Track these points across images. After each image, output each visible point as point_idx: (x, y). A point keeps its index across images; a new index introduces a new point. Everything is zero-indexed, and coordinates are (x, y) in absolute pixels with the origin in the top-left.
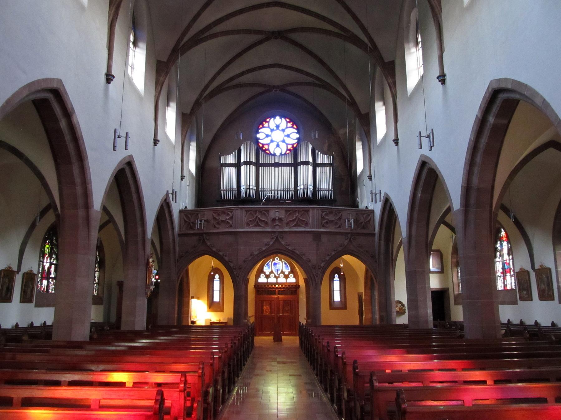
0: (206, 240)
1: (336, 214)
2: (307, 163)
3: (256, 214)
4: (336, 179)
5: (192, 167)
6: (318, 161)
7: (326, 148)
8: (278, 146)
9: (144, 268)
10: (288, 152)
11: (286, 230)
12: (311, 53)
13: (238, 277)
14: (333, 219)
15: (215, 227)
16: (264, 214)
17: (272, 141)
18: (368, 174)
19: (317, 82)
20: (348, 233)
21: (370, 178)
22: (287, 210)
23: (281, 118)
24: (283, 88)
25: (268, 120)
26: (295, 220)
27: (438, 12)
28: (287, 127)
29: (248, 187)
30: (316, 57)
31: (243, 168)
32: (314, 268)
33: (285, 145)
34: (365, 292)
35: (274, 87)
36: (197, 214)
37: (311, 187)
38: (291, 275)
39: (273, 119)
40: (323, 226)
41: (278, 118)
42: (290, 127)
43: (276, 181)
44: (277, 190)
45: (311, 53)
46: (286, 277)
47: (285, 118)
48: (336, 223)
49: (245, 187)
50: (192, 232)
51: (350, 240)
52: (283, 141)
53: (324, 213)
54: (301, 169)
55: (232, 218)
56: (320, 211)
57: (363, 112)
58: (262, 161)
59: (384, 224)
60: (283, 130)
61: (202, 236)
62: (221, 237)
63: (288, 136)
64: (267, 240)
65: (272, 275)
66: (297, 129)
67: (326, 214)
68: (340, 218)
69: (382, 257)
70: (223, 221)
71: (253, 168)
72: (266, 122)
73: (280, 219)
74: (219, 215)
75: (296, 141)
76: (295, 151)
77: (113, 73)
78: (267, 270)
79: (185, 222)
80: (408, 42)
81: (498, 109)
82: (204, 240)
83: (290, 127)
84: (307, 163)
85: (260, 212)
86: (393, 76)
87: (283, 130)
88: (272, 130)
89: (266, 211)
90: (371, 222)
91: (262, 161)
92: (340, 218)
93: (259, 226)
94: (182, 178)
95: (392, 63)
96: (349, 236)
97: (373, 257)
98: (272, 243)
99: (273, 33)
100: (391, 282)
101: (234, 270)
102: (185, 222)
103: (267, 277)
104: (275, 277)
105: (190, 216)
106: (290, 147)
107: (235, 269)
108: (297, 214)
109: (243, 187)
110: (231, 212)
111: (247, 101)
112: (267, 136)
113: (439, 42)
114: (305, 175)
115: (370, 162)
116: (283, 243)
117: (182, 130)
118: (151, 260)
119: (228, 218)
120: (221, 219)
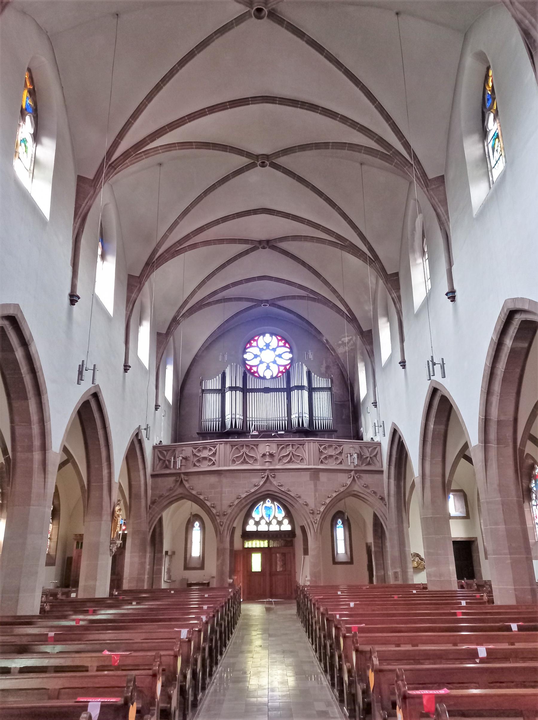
0: (184, 482)
1: (336, 448)
2: (301, 388)
5: (169, 393)
6: (315, 385)
7: (323, 370)
8: (268, 367)
9: (109, 518)
10: (280, 374)
12: (304, 264)
13: (221, 526)
15: (195, 465)
16: (252, 448)
17: (261, 362)
19: (311, 296)
20: (351, 470)
21: (375, 404)
25: (256, 338)
26: (288, 455)
27: (445, 222)
28: (278, 346)
30: (310, 268)
31: (228, 394)
32: (313, 513)
34: (374, 542)
35: (262, 301)
36: (174, 450)
37: (306, 416)
38: (286, 521)
39: (262, 337)
40: (322, 462)
41: (268, 335)
43: (266, 410)
44: (267, 420)
45: (304, 264)
46: (280, 523)
47: (276, 335)
48: (337, 458)
49: (230, 416)
50: (168, 471)
51: (354, 479)
52: (275, 362)
53: (323, 447)
54: (295, 394)
55: (214, 454)
56: (317, 445)
57: (364, 329)
58: (250, 386)
59: (394, 459)
60: (274, 350)
61: (180, 478)
62: (201, 477)
63: (280, 356)
65: (263, 522)
66: (290, 348)
67: (325, 448)
68: (341, 453)
69: (393, 500)
70: (205, 458)
71: (239, 394)
72: (254, 340)
73: (271, 455)
74: (199, 451)
75: (289, 361)
76: (287, 373)
77: (78, 293)
79: (160, 459)
80: (414, 251)
81: (516, 331)
82: (182, 480)
84: (301, 388)
85: (247, 446)
86: (371, 343)
88: (261, 350)
89: (254, 445)
91: (250, 386)
92: (341, 453)
93: (247, 463)
94: (157, 407)
95: (370, 331)
96: (353, 472)
97: (382, 499)
98: (261, 483)
99: (260, 242)
100: (405, 530)
101: (217, 517)
102: (160, 459)
103: (257, 523)
104: (267, 523)
105: (165, 453)
106: (282, 369)
107: (218, 516)
108: (291, 449)
109: (228, 417)
110: (214, 447)
111: (232, 317)
112: (256, 356)
113: (447, 255)
114: (300, 402)
115: (375, 386)
116: (275, 483)
117: (157, 353)
118: (117, 508)
119: (210, 454)
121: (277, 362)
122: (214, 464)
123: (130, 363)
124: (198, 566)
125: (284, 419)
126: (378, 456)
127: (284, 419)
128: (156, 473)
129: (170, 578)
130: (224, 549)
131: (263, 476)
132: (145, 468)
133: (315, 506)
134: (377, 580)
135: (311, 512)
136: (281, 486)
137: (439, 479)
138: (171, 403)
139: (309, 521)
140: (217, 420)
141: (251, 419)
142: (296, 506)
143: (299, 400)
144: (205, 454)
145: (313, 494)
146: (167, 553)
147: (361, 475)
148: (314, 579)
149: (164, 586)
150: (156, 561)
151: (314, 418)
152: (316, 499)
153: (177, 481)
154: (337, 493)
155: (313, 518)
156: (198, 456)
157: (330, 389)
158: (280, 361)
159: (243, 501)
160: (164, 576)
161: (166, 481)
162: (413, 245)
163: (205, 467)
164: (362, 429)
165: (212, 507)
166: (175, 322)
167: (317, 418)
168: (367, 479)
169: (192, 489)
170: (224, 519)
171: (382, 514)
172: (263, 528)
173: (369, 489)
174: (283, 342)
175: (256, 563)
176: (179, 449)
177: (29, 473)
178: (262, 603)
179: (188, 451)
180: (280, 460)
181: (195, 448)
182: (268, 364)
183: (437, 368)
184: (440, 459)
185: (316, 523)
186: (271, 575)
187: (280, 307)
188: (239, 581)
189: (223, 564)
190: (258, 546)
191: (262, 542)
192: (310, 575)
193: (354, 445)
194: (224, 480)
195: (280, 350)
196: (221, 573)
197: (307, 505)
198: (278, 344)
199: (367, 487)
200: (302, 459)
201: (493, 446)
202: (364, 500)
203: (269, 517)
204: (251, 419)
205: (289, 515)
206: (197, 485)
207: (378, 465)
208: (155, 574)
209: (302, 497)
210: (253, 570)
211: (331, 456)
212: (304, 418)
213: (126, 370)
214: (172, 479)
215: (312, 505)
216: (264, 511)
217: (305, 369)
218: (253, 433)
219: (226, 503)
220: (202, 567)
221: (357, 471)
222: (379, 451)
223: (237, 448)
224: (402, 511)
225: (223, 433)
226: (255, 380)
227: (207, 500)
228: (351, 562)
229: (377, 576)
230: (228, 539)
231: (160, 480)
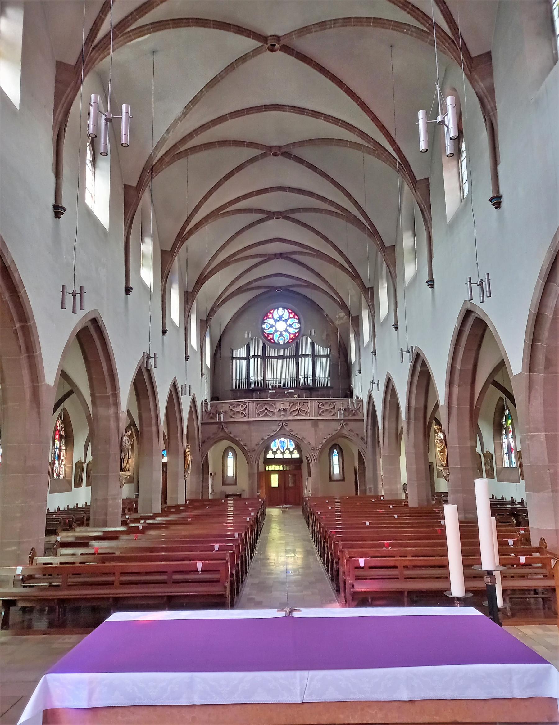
2: (306, 356)
4: (333, 367)
5: (208, 361)
6: (317, 353)
7: (324, 337)
8: (281, 335)
9: (183, 457)
11: (289, 418)
15: (231, 417)
23: (284, 309)
24: (286, 289)
25: (272, 312)
28: (289, 318)
29: (256, 378)
31: (252, 361)
32: (313, 450)
33: (288, 335)
35: (276, 288)
36: (216, 407)
38: (296, 451)
39: (276, 310)
41: (281, 309)
42: (292, 318)
43: (280, 372)
46: (291, 453)
47: (287, 309)
48: (331, 412)
52: (286, 331)
54: (301, 360)
55: (245, 409)
58: (268, 354)
61: (221, 426)
62: (236, 425)
63: (290, 326)
65: (279, 452)
66: (299, 319)
69: (370, 440)
70: (238, 412)
71: (260, 361)
72: (270, 313)
73: (285, 410)
74: (234, 407)
75: (298, 330)
77: (167, 328)
78: (274, 446)
80: (382, 278)
83: (292, 318)
84: (306, 356)
87: (286, 321)
88: (276, 321)
90: (361, 409)
91: (268, 354)
92: (334, 408)
96: (342, 422)
97: (362, 439)
98: (278, 430)
99: (275, 255)
103: (275, 453)
104: (282, 453)
112: (272, 326)
118: (187, 450)
121: (289, 331)
124: (233, 483)
128: (204, 422)
129: (213, 491)
130: (254, 474)
134: (360, 492)
137: (394, 431)
138: (209, 366)
143: (305, 365)
144: (239, 409)
146: (211, 474)
149: (210, 497)
150: (205, 480)
153: (219, 428)
157: (328, 356)
158: (291, 330)
160: (210, 490)
161: (213, 429)
162: (381, 274)
163: (238, 418)
166: (213, 311)
168: (352, 425)
170: (253, 454)
172: (279, 456)
175: (275, 481)
176: (220, 405)
177: (151, 439)
179: (226, 407)
180: (291, 413)
181: (231, 405)
182: (281, 332)
183: (375, 386)
184: (394, 419)
186: (285, 488)
187: (290, 291)
188: (262, 493)
190: (276, 469)
191: (278, 467)
194: (252, 428)
195: (290, 322)
196: (252, 490)
197: (310, 444)
199: (352, 431)
201: (412, 421)
202: (350, 440)
203: (283, 448)
205: (298, 448)
206: (234, 430)
207: (361, 415)
208: (205, 488)
210: (272, 486)
213: (187, 359)
215: (313, 444)
216: (279, 444)
217: (310, 341)
218: (271, 391)
220: (236, 484)
221: (345, 420)
222: (361, 407)
225: (251, 391)
228: (343, 480)
231: (207, 427)
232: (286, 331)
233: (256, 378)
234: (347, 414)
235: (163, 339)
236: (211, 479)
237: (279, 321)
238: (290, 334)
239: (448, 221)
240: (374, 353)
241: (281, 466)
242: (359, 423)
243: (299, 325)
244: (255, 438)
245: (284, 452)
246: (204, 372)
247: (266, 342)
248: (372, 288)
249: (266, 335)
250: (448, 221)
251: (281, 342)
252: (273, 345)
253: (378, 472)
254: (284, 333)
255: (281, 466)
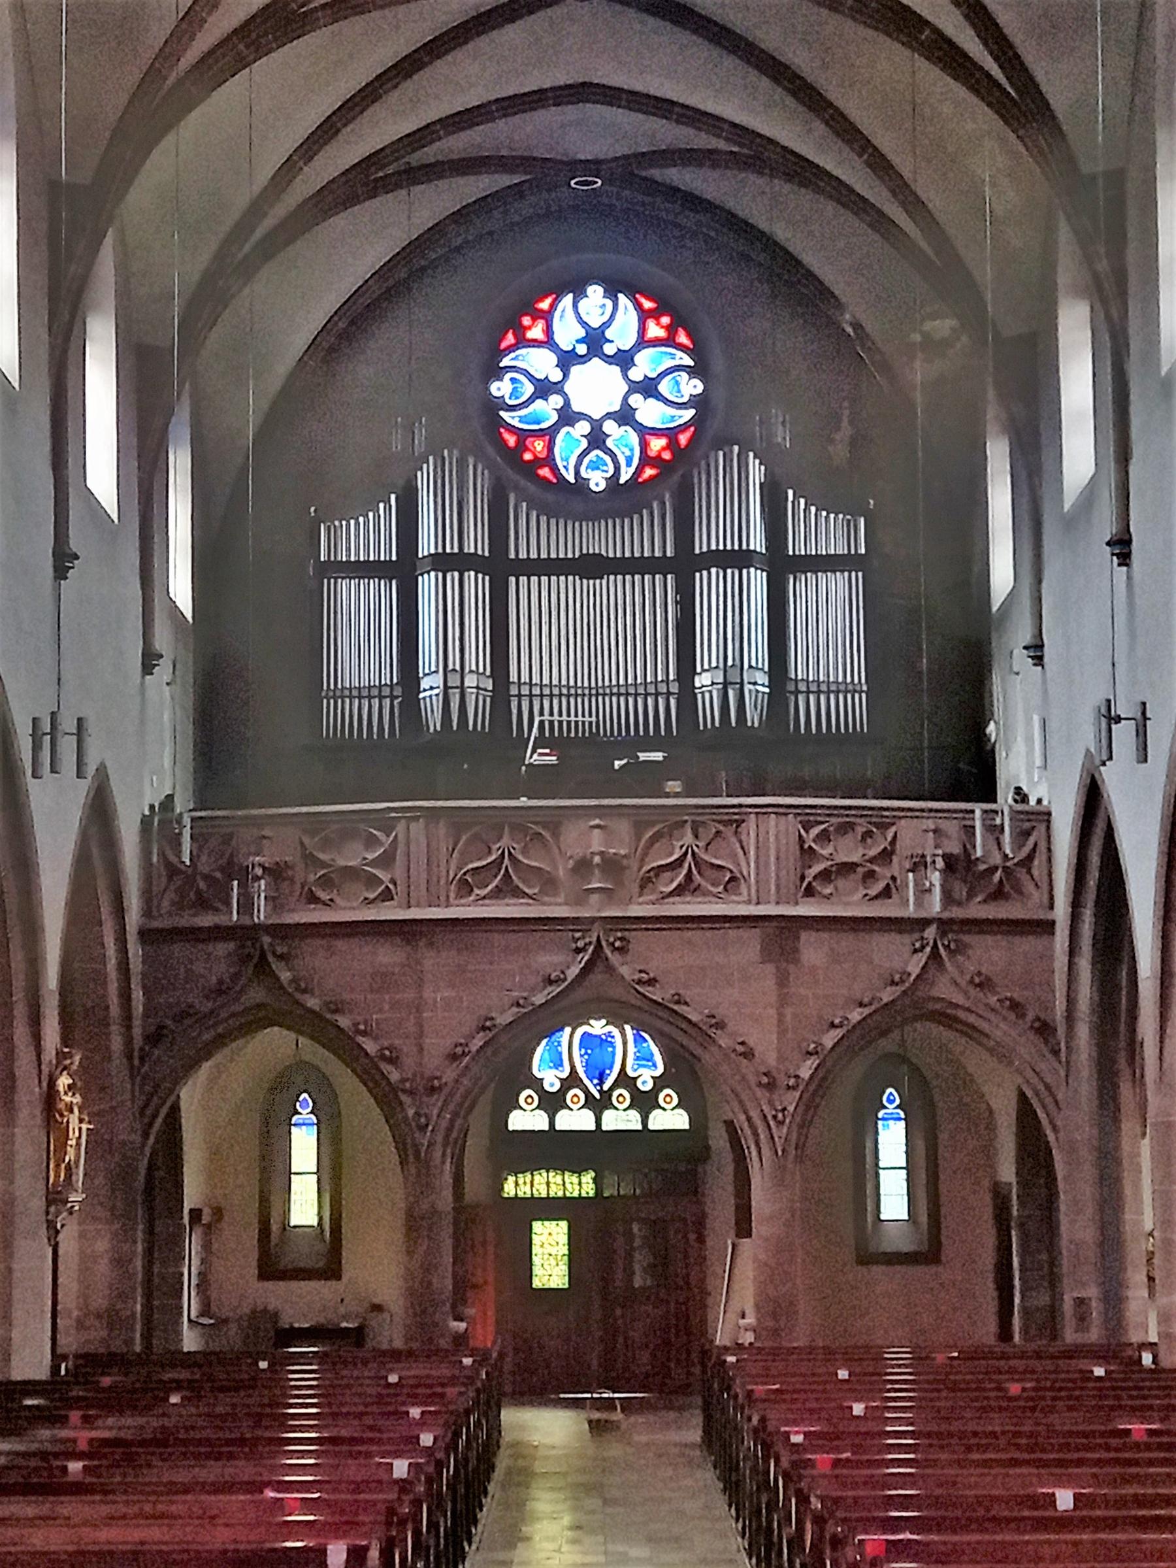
1: (868, 834)
2: (740, 559)
3: (500, 838)
5: (180, 586)
6: (797, 545)
8: (597, 439)
13: (423, 1128)
14: (855, 858)
15: (313, 899)
18: (1025, 635)
20: (924, 923)
22: (640, 819)
23: (611, 293)
25: (545, 305)
26: (680, 861)
28: (643, 342)
29: (454, 681)
31: (427, 584)
32: (771, 1086)
33: (634, 438)
39: (568, 299)
40: (810, 892)
41: (595, 292)
42: (656, 342)
44: (597, 693)
46: (645, 1102)
47: (632, 292)
48: (870, 875)
49: (438, 680)
50: (206, 920)
51: (935, 955)
54: (711, 586)
56: (792, 824)
58: (522, 548)
60: (624, 360)
61: (256, 949)
62: (340, 944)
63: (648, 388)
64: (550, 959)
67: (824, 837)
68: (886, 855)
69: (1083, 1032)
70: (351, 873)
71: (476, 585)
72: (538, 315)
73: (612, 866)
74: (326, 844)
75: (689, 414)
84: (740, 559)
87: (624, 360)
88: (567, 360)
89: (545, 825)
92: (886, 855)
93: (517, 893)
94: (149, 661)
96: (931, 932)
97: (1044, 1029)
98: (573, 972)
103: (552, 1103)
107: (411, 1093)
108: (689, 838)
109: (431, 684)
112: (544, 389)
116: (624, 971)
118: (64, 1081)
119: (370, 856)
120: (342, 862)
121: (639, 416)
122: (387, 896)
123: (74, 545)
125: (663, 688)
126: (1036, 862)
127: (663, 688)
128: (156, 924)
129: (205, 1311)
131: (580, 944)
132: (120, 911)
133: (781, 1058)
135: (765, 1080)
136: (652, 982)
138: (189, 615)
139: (755, 1114)
140: (386, 691)
141: (525, 690)
142: (706, 1057)
143: (734, 608)
144: (352, 856)
145: (772, 1012)
146: (196, 1214)
147: (966, 938)
148: (770, 1323)
149: (190, 1341)
151: (791, 687)
152: (782, 1033)
154: (867, 1011)
155: (771, 1103)
156: (323, 865)
158: (650, 413)
159: (503, 1039)
160: (190, 1303)
164: (991, 728)
165: (383, 1058)
166: (210, 297)
167: (802, 687)
168: (989, 954)
169: (305, 991)
171: (1041, 1087)
172: (575, 1119)
173: (995, 993)
174: (665, 320)
175: (550, 1255)
178: (576, 1404)
180: (646, 882)
181: (313, 833)
183: (1124, 733)
185: (781, 1123)
189: (428, 1268)
190: (556, 1191)
191: (571, 1179)
192: (757, 1307)
193: (944, 825)
196: (421, 1299)
197: (749, 1054)
198: (642, 330)
200: (733, 879)
202: (972, 1032)
204: (525, 690)
205: (683, 1074)
207: (1037, 897)
209: (731, 1026)
210: (537, 1283)
211: (848, 868)
212: (747, 687)
213: (61, 572)
214: (222, 949)
217: (756, 472)
219: (437, 1045)
220: (331, 1270)
221: (945, 925)
222: (1043, 846)
223: (476, 837)
224: (1116, 1074)
226: (543, 519)
227: (364, 1033)
228: (929, 1254)
229: (1025, 1311)
230: (448, 1178)
232: (625, 416)
233: (454, 681)
234: (960, 890)
235: (142, 684)
236: (193, 1246)
237: (583, 359)
238: (645, 433)
239: (1067, 507)
240: (1122, 547)
241: (588, 1178)
242: (1028, 944)
243: (694, 387)
244: (444, 1011)
245: (607, 1095)
246: (163, 640)
247: (510, 473)
248: (1117, 178)
249: (511, 440)
250: (1067, 507)
251: (597, 481)
252: (550, 497)
253: (1128, 1216)
254: (609, 427)
255: (588, 1178)
